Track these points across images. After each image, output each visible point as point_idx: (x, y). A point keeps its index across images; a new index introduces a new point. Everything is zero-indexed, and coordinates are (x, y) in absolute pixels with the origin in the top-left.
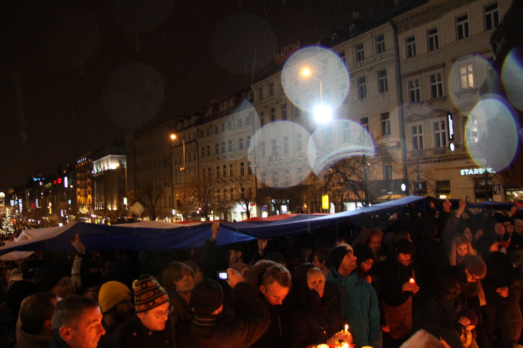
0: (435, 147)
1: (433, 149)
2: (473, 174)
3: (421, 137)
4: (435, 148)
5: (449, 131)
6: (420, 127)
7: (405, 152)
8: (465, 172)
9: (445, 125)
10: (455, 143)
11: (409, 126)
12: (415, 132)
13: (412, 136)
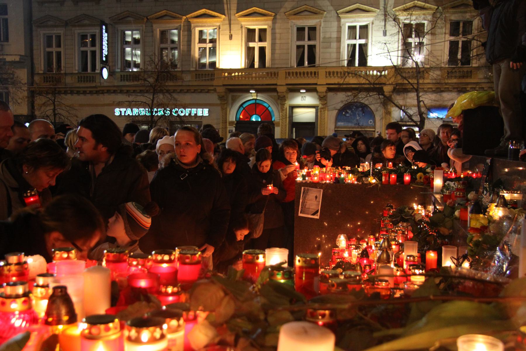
0: (80, 71)
1: (75, 74)
2: (131, 114)
3: (59, 54)
4: (79, 73)
5: (102, 49)
6: (59, 37)
7: (32, 73)
8: (121, 112)
9: (96, 40)
10: (109, 68)
11: (40, 34)
12: (49, 45)
13: (44, 49)
